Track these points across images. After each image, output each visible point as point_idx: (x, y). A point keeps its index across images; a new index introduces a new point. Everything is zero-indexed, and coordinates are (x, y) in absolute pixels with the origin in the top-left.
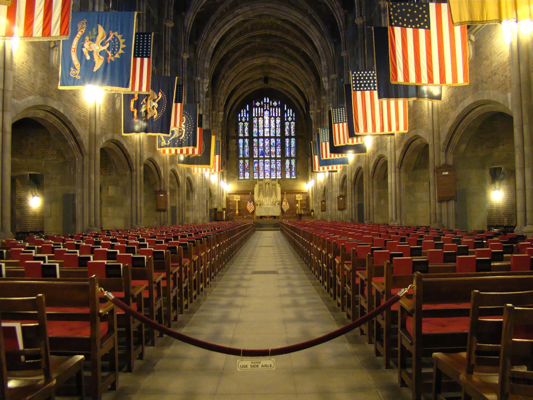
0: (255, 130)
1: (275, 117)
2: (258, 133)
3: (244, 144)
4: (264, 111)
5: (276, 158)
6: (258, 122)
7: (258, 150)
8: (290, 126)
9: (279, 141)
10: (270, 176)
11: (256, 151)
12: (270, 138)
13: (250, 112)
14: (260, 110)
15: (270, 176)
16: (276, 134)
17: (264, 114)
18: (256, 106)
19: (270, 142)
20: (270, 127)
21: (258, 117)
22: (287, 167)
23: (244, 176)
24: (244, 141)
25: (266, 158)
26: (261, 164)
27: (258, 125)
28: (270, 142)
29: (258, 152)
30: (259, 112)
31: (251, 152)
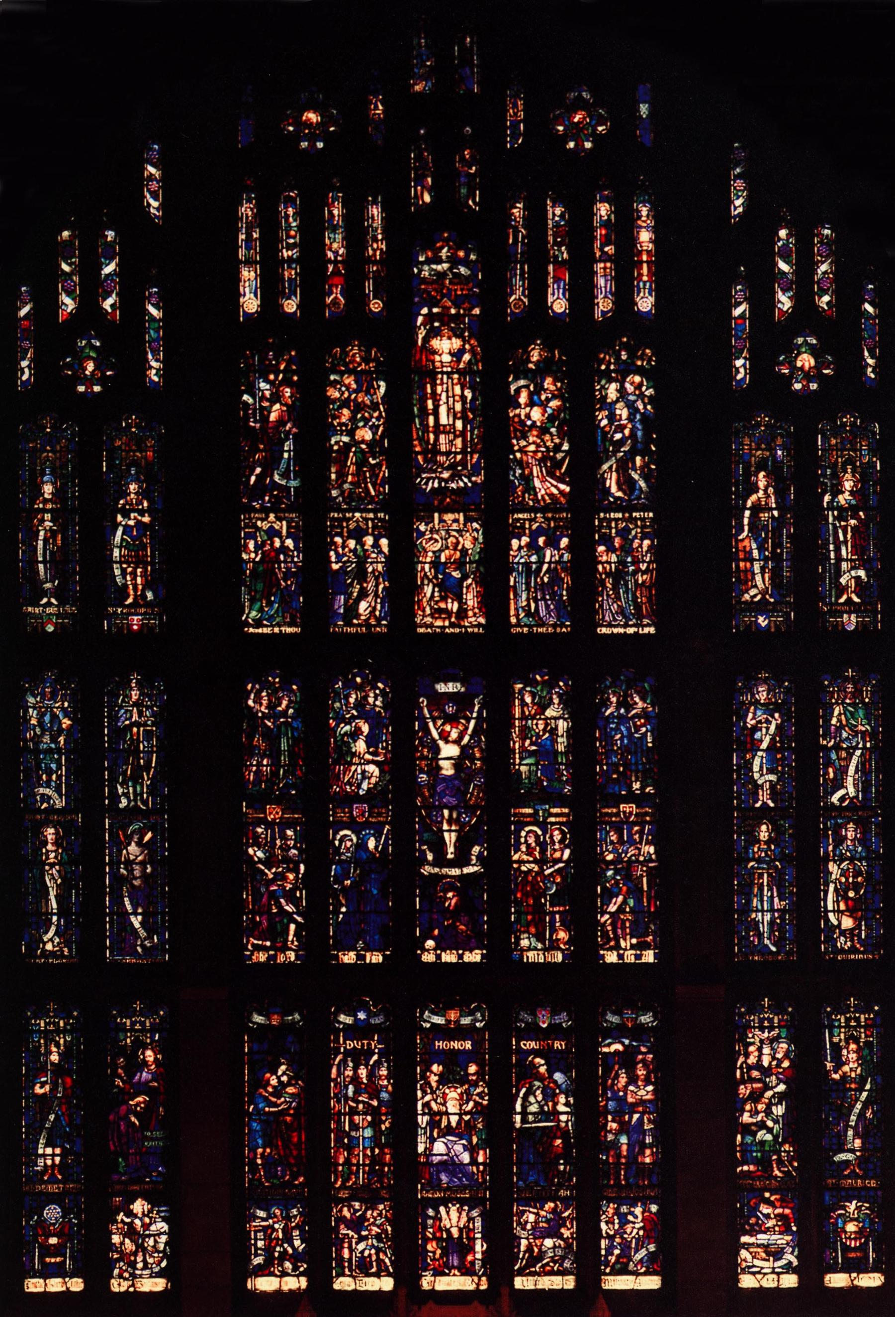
0: (268, 537)
1: (580, 350)
2: (318, 584)
3: (93, 755)
4: (411, 232)
5: (584, 986)
6: (312, 415)
7: (318, 850)
8: (803, 486)
9: (632, 714)
10: (502, 1261)
11: (271, 846)
12: (494, 662)
13: (188, 261)
14: (351, 231)
15: (502, 1261)
16: (582, 586)
17: (403, 290)
18: (279, 170)
19: (496, 730)
20: (494, 504)
21: (310, 346)
22: (764, 1117)
23: (95, 1261)
24: (90, 712)
25: (450, 986)
26: (357, 1076)
27: (315, 457)
28: (496, 730)
29: (316, 882)
30: (336, 245)
31: (204, 880)
